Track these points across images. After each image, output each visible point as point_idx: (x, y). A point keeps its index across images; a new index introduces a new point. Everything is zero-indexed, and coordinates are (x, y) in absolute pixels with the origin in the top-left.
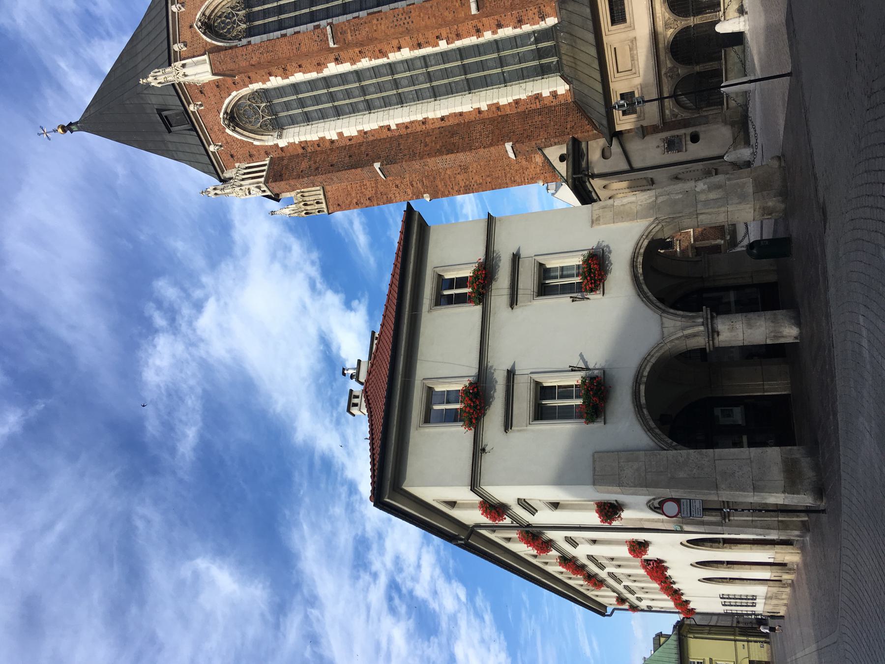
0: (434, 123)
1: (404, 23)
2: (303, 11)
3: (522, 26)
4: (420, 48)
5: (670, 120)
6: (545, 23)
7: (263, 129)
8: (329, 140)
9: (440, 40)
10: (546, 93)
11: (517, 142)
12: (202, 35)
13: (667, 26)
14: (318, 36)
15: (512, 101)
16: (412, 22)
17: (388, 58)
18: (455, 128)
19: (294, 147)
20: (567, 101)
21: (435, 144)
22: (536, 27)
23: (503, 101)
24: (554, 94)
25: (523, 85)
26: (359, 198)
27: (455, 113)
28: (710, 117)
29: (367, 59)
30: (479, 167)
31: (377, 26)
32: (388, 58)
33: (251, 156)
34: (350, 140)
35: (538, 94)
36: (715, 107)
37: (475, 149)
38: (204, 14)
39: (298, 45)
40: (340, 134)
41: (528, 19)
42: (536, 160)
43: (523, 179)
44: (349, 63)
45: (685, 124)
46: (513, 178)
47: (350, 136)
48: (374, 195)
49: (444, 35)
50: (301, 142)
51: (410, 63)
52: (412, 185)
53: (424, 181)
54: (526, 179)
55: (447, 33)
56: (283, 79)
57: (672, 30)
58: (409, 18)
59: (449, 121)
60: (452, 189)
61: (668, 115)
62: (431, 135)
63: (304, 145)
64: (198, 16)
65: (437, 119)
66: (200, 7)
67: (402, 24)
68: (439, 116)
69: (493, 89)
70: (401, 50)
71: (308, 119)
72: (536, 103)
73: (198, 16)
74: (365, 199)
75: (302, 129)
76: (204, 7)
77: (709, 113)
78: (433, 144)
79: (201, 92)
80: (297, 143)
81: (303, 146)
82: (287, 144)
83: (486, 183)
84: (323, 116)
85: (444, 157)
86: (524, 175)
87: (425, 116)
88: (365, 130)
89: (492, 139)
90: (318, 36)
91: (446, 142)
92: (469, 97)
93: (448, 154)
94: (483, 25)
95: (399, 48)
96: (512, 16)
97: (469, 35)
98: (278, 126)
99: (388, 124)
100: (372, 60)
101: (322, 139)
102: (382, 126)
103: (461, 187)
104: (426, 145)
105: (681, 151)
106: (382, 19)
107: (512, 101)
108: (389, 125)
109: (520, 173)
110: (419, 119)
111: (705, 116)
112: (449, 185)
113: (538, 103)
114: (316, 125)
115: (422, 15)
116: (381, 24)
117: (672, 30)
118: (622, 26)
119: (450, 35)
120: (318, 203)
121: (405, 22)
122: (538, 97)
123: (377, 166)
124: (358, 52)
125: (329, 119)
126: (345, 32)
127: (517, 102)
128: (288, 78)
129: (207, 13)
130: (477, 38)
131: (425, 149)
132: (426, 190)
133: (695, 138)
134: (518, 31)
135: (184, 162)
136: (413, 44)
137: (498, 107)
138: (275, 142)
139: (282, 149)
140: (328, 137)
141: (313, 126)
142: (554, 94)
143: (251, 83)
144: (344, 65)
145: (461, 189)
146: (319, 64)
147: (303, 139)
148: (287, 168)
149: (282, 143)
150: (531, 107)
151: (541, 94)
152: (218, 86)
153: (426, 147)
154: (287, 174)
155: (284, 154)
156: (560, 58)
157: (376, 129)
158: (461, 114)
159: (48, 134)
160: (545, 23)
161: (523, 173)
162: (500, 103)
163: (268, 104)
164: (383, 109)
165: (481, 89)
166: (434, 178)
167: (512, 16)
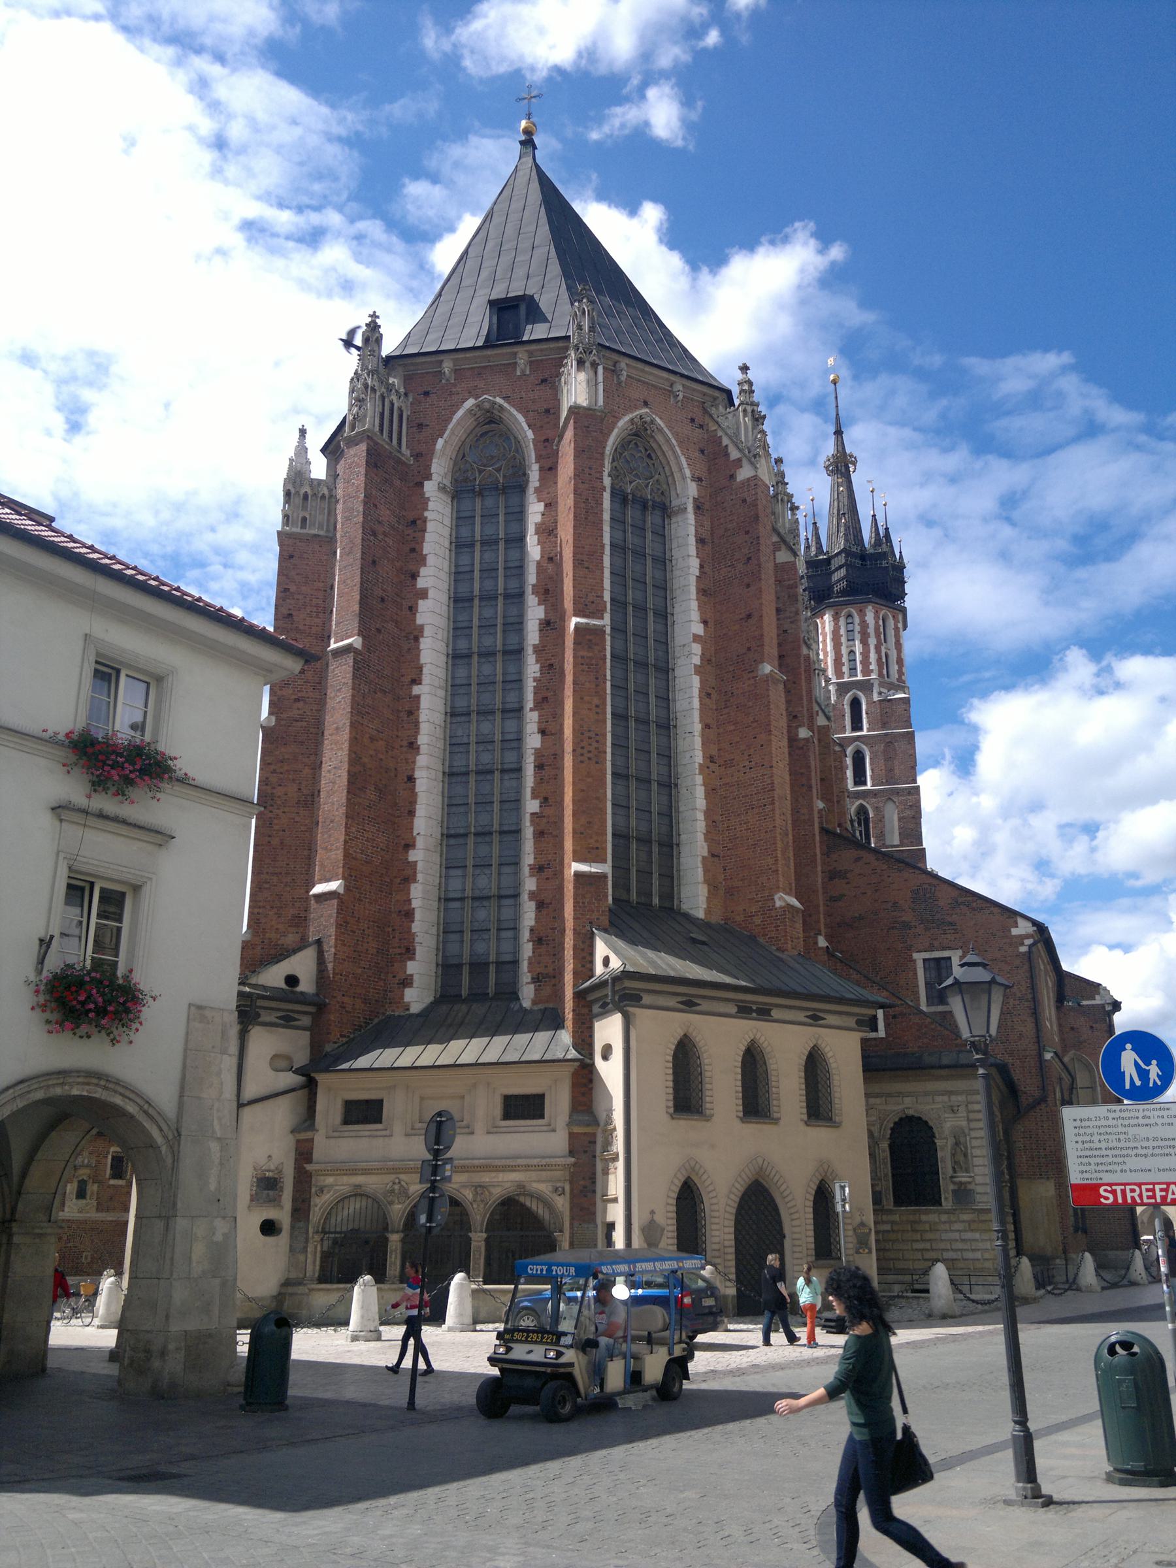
0: (407, 763)
3: (531, 943)
4: (535, 766)
5: (313, 1182)
6: (527, 983)
7: (460, 460)
8: (419, 572)
9: (541, 803)
10: (412, 967)
11: (342, 902)
12: (631, 416)
13: (479, 1188)
14: (593, 602)
15: (413, 906)
16: (582, 762)
17: (531, 710)
18: (390, 797)
19: (419, 507)
20: (390, 1003)
21: (371, 756)
22: (524, 966)
24: (407, 982)
25: (434, 931)
26: (296, 596)
27: (416, 802)
28: (302, 1258)
29: (538, 675)
30: (303, 828)
31: (589, 703)
32: (531, 710)
33: (420, 426)
34: (411, 608)
35: (414, 954)
36: (318, 1268)
37: (346, 824)
38: (660, 430)
39: (586, 565)
40: (423, 594)
41: (540, 956)
42: (290, 935)
43: (261, 904)
44: (537, 642)
45: (300, 1210)
46: (267, 886)
47: (417, 611)
48: (294, 626)
49: (548, 811)
50: (425, 520)
51: (514, 744)
52: (297, 700)
53: (299, 724)
54: (261, 911)
55: (549, 817)
56: (536, 524)
57: (470, 1196)
58: (589, 759)
59: (404, 790)
60: (274, 772)
61: (324, 1181)
63: (417, 524)
64: (658, 420)
65: (413, 770)
66: (671, 428)
67: (582, 745)
68: (417, 774)
69: (440, 877)
70: (540, 735)
72: (400, 947)
73: (658, 420)
74: (291, 607)
75: (446, 532)
76: (670, 436)
77: (309, 1256)
78: (372, 752)
79: (544, 381)
80: (426, 514)
81: (418, 522)
82: (426, 496)
83: (270, 836)
84: (459, 575)
85: (346, 766)
86: (268, 907)
87: (424, 749)
89: (355, 859)
90: (593, 602)
91: (370, 776)
92: (437, 832)
93: (349, 774)
94: (547, 879)
95: (543, 732)
96: (551, 929)
97: (538, 852)
98: (459, 491)
99: (423, 683)
100: (534, 681)
101: (422, 560)
102: (421, 671)
103: (274, 788)
104: (372, 739)
105: (252, 1200)
106: (597, 713)
107: (413, 906)
108: (420, 684)
109: (273, 901)
110: (419, 737)
111: (305, 1248)
112: (281, 767)
113: (398, 951)
114: (447, 558)
115: (589, 780)
116: (590, 709)
117: (470, 1196)
118: (498, 1111)
119: (545, 820)
120: (304, 520)
121: (585, 751)
122: (409, 952)
123: (354, 640)
124: (552, 662)
125: (453, 583)
126: (590, 647)
127: (409, 915)
128: (536, 534)
129: (659, 438)
130: (529, 865)
131: (368, 736)
132: (283, 723)
133: (268, 1228)
134: (526, 935)
135: (431, 313)
136: (543, 756)
138: (434, 476)
139: (421, 485)
140: (423, 571)
141: (448, 552)
142: (407, 982)
143: (541, 469)
144: (537, 634)
145: (269, 787)
146: (547, 591)
147: (430, 526)
148: (386, 480)
149: (430, 488)
150: (394, 937)
151: (412, 958)
152: (548, 411)
153: (370, 738)
154: (376, 478)
155: (411, 484)
156: (464, 1001)
157: (418, 659)
158: (412, 813)
159: (526, 101)
160: (527, 983)
161: (272, 907)
162: (416, 885)
163: (500, 486)
164: (450, 680)
165: (444, 856)
166: (302, 743)
167: (551, 929)
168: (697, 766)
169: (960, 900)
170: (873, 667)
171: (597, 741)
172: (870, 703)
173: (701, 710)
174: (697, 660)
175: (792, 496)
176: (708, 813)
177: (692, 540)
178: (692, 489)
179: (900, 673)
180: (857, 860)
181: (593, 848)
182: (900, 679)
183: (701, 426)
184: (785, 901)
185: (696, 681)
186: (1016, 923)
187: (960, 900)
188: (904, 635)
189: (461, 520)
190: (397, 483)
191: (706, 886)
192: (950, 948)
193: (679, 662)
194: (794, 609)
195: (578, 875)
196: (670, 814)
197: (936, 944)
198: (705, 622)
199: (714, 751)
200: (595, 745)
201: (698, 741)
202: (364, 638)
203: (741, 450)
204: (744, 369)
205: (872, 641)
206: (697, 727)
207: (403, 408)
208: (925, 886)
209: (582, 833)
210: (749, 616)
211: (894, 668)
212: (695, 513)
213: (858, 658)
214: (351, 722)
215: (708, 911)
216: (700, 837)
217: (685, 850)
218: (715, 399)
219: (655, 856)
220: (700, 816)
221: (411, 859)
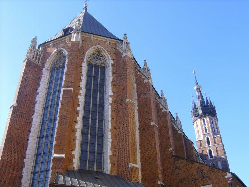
1: (61, 121)
2: (92, 87)
21: (16, 134)
23: (24, 170)
25: (29, 182)
40: (38, 94)
50: (41, 77)
62: (22, 133)
65: (28, 137)
67: (61, 120)
71: (50, 82)
75: (47, 79)
76: (105, 50)
87: (32, 131)
88: (36, 104)
99: (35, 114)
115: (62, 130)
121: (62, 122)
127: (21, 177)
129: (103, 52)
137: (23, 167)
139: (42, 70)
140: (39, 88)
158: (26, 149)
168: (109, 129)
169: (210, 170)
170: (211, 130)
171: (66, 119)
172: (211, 138)
173: (111, 114)
174: (111, 102)
175: (148, 67)
176: (112, 143)
177: (111, 73)
178: (112, 62)
179: (218, 131)
180: (182, 163)
181: (61, 150)
182: (218, 132)
183: (115, 49)
184: (131, 165)
185: (110, 107)
186: (226, 174)
187: (210, 170)
188: (219, 123)
189: (52, 76)
190: (36, 70)
191: (111, 164)
192: (209, 184)
193: (106, 103)
194: (149, 93)
195: (55, 158)
196: (101, 145)
197: (205, 183)
198: (114, 92)
199: (115, 125)
200: (65, 120)
201: (110, 123)
202: (18, 104)
203: (123, 51)
204: (125, 34)
205: (209, 124)
206: (110, 119)
207: (41, 54)
208: (200, 167)
209: (58, 146)
210: (124, 88)
211: (216, 130)
212: (112, 67)
213: (207, 128)
214: (9, 124)
215: (111, 172)
216: (109, 150)
217: (105, 154)
218: (119, 42)
219: (96, 156)
220: (110, 144)
221: (24, 161)
